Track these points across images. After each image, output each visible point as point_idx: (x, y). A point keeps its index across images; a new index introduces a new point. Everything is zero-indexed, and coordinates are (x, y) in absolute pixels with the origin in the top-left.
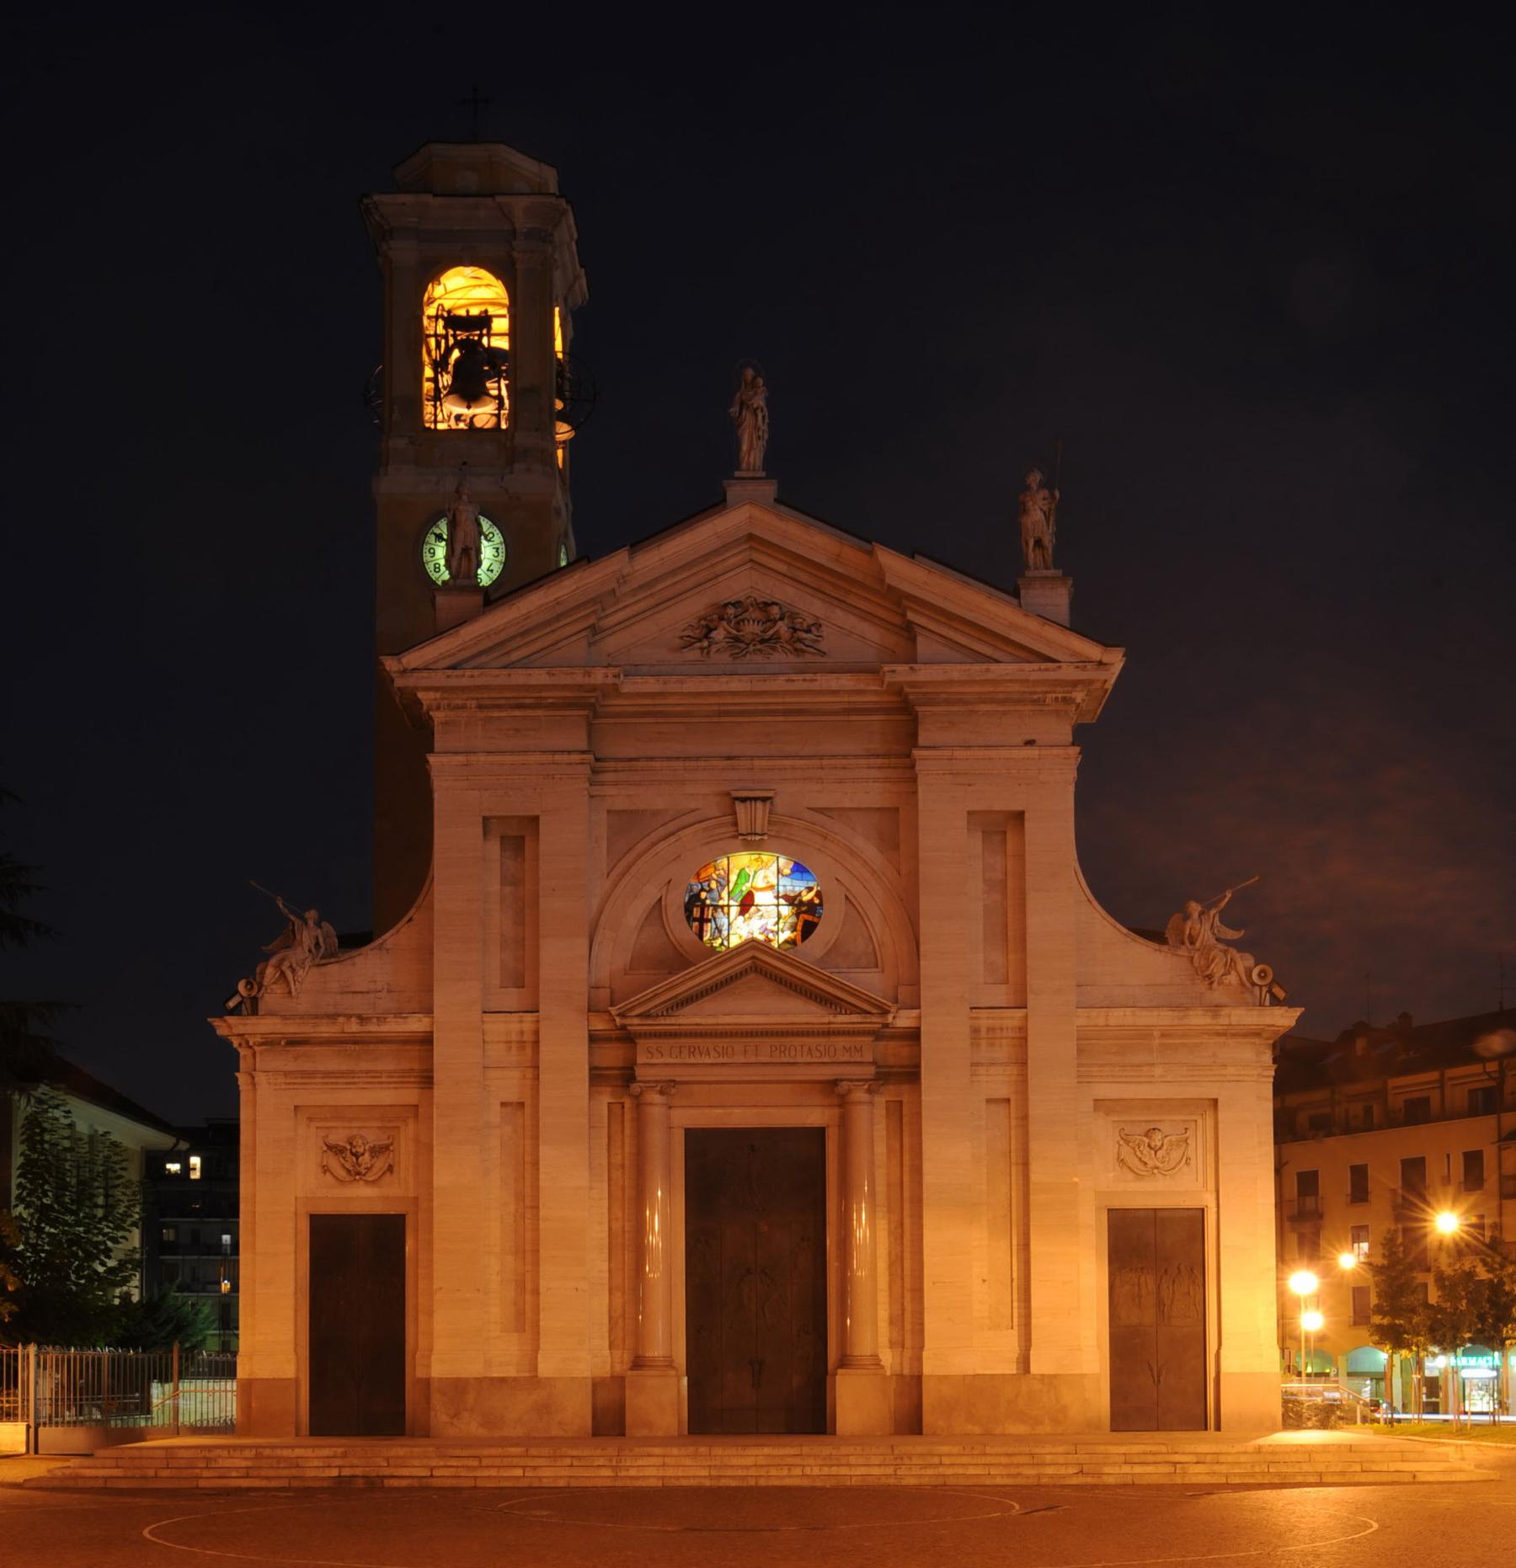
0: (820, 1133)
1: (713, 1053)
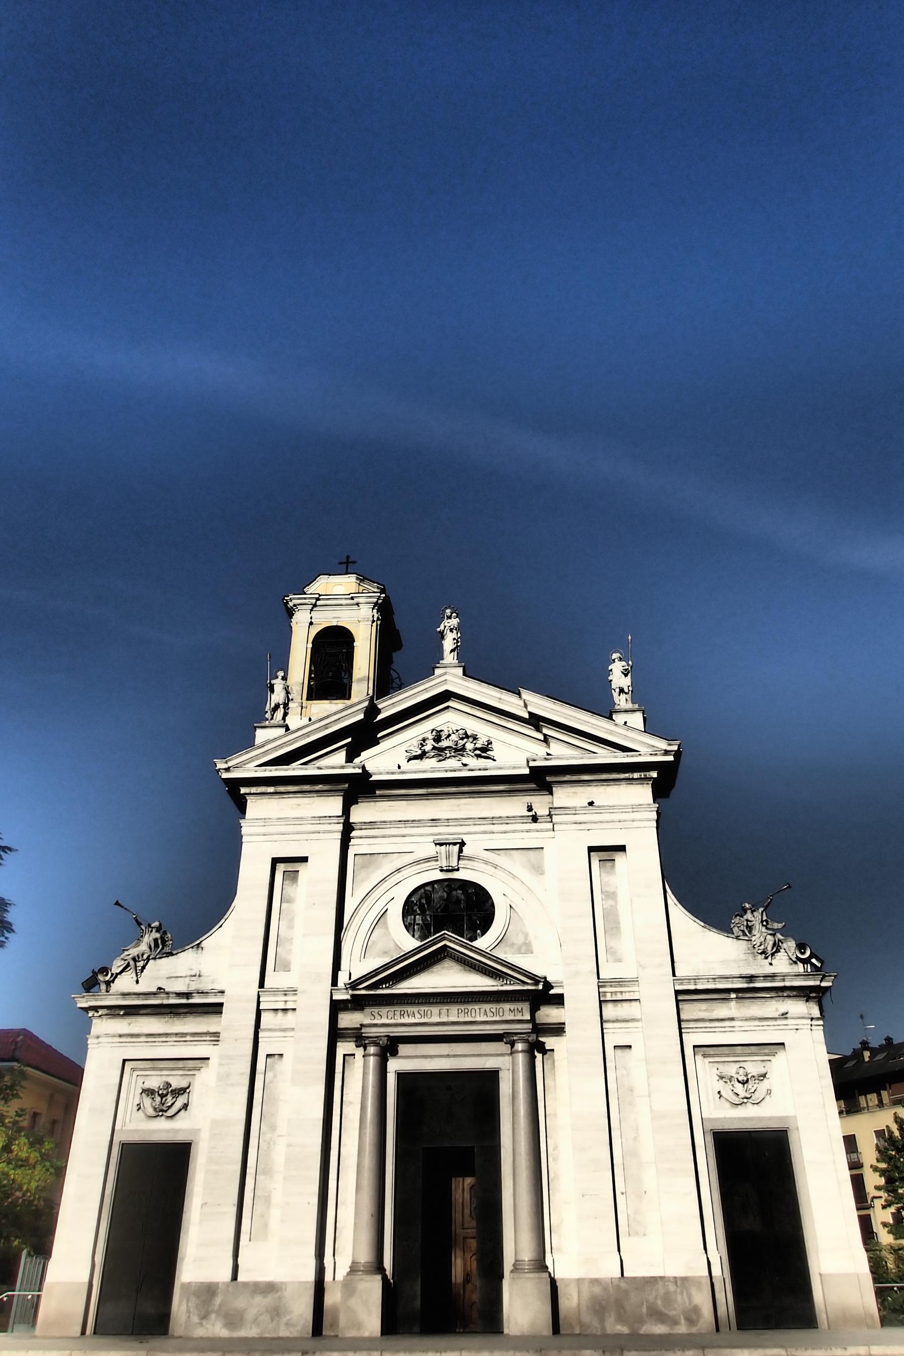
1: (417, 1015)
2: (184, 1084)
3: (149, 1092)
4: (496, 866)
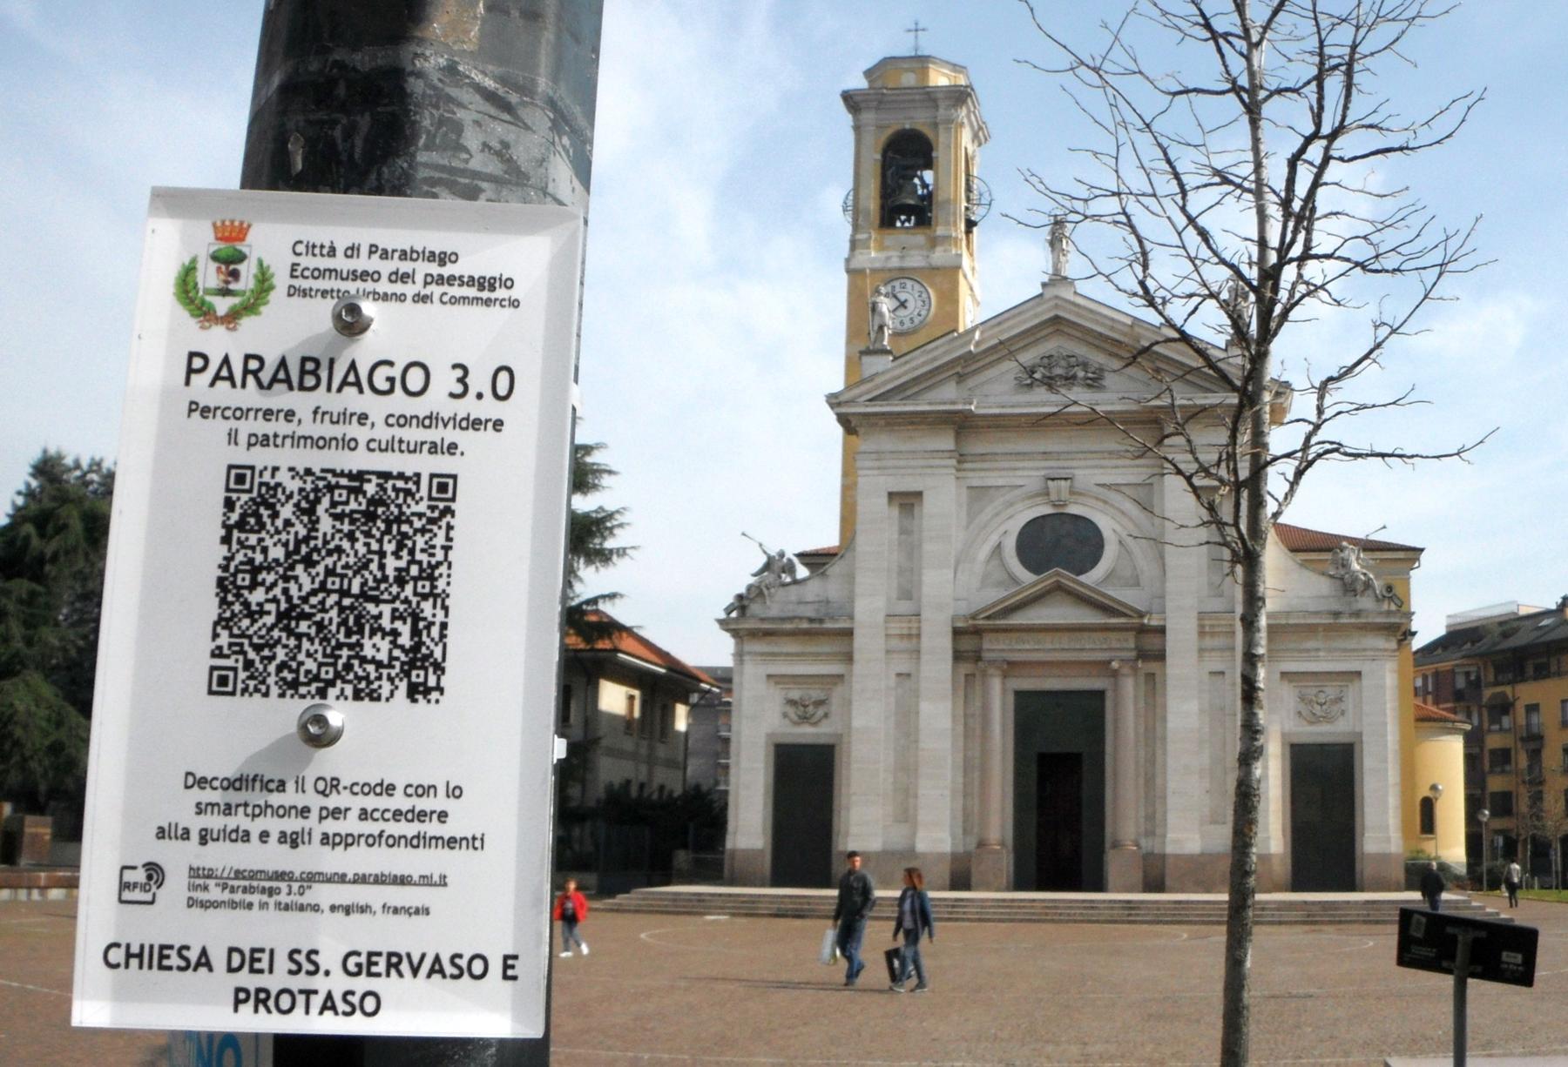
0: (1100, 695)
2: (822, 696)
3: (792, 702)
4: (1105, 502)
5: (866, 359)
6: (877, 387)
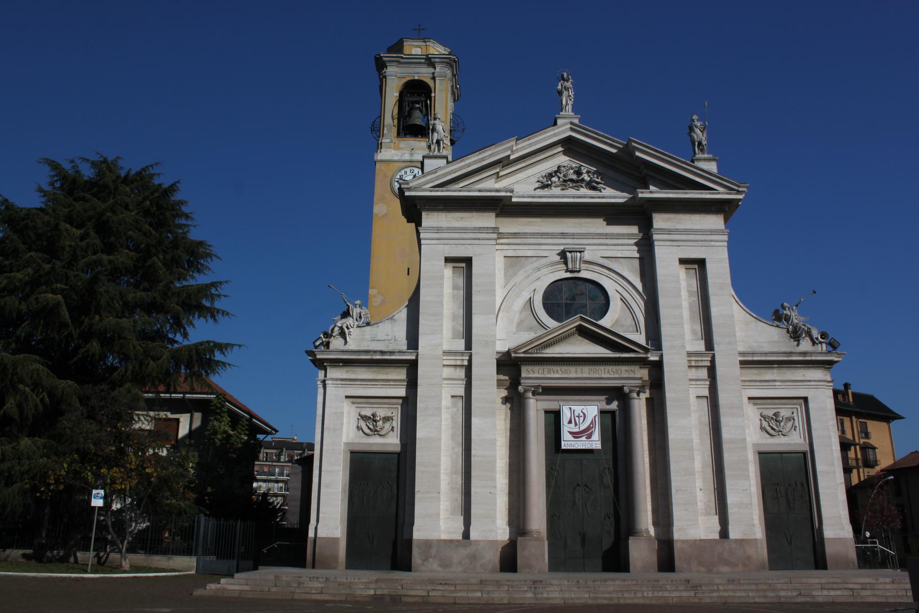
2: (389, 414)
3: (364, 418)
5: (426, 161)
6: (438, 178)
